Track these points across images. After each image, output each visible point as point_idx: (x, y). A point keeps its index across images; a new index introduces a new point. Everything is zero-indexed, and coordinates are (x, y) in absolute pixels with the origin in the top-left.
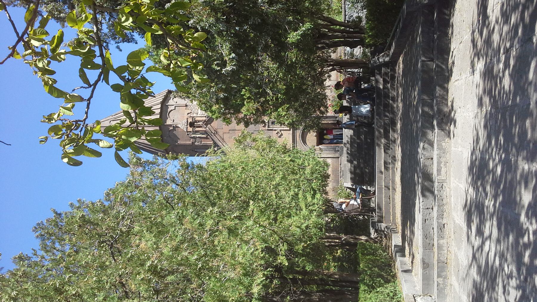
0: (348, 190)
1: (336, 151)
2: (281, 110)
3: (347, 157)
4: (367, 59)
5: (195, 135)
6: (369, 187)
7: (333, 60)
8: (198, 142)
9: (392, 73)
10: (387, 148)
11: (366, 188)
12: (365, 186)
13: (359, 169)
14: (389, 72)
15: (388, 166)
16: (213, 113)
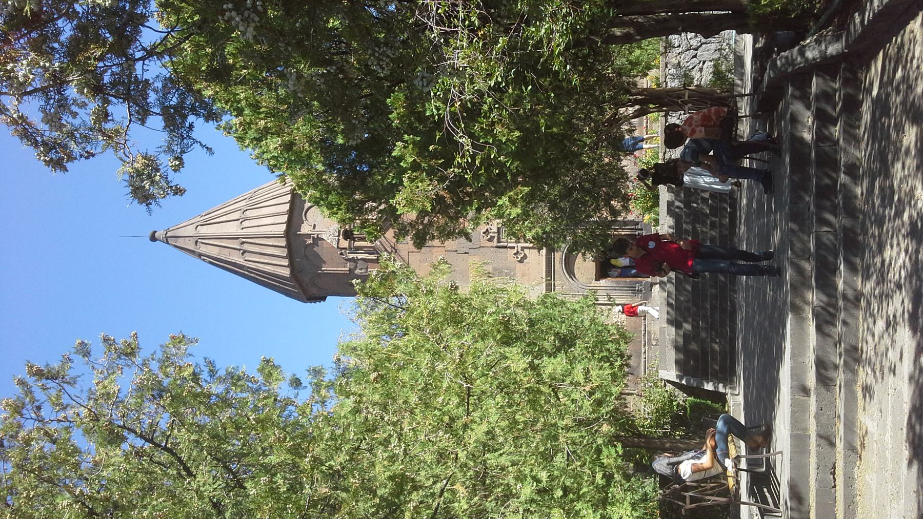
0: (669, 387)
2: (507, 203)
3: (668, 313)
4: (724, 86)
5: (355, 256)
6: (721, 385)
7: (643, 91)
8: (361, 269)
9: (850, 91)
10: (828, 318)
11: (715, 387)
12: (711, 384)
13: (696, 342)
14: (835, 91)
15: (831, 374)
16: (335, 209)
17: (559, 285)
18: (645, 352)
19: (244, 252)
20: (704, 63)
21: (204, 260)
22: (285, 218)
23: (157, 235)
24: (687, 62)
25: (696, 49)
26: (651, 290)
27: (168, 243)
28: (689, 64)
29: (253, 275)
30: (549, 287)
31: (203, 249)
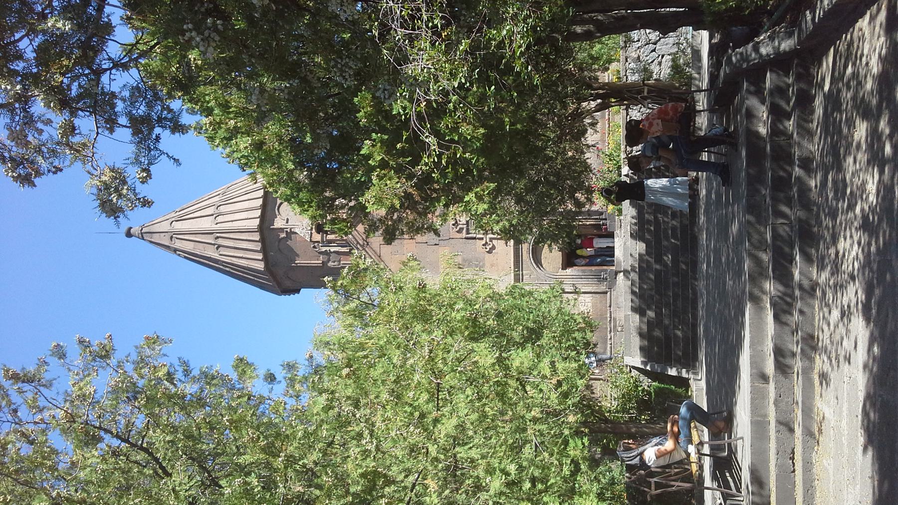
0: (634, 373)
1: (600, 280)
2: (474, 199)
3: (632, 301)
4: (682, 80)
5: (328, 249)
6: (684, 371)
7: (604, 86)
8: (334, 262)
9: (803, 86)
10: (785, 307)
11: (678, 373)
12: (674, 369)
13: (659, 329)
14: (789, 86)
15: (789, 361)
16: (306, 206)
17: (527, 274)
18: (611, 339)
19: (219, 246)
20: (663, 56)
21: (179, 255)
22: (258, 213)
23: (132, 231)
24: (646, 56)
25: (655, 43)
26: (616, 278)
27: (143, 239)
28: (648, 58)
29: (227, 269)
30: (517, 278)
31: (178, 244)
